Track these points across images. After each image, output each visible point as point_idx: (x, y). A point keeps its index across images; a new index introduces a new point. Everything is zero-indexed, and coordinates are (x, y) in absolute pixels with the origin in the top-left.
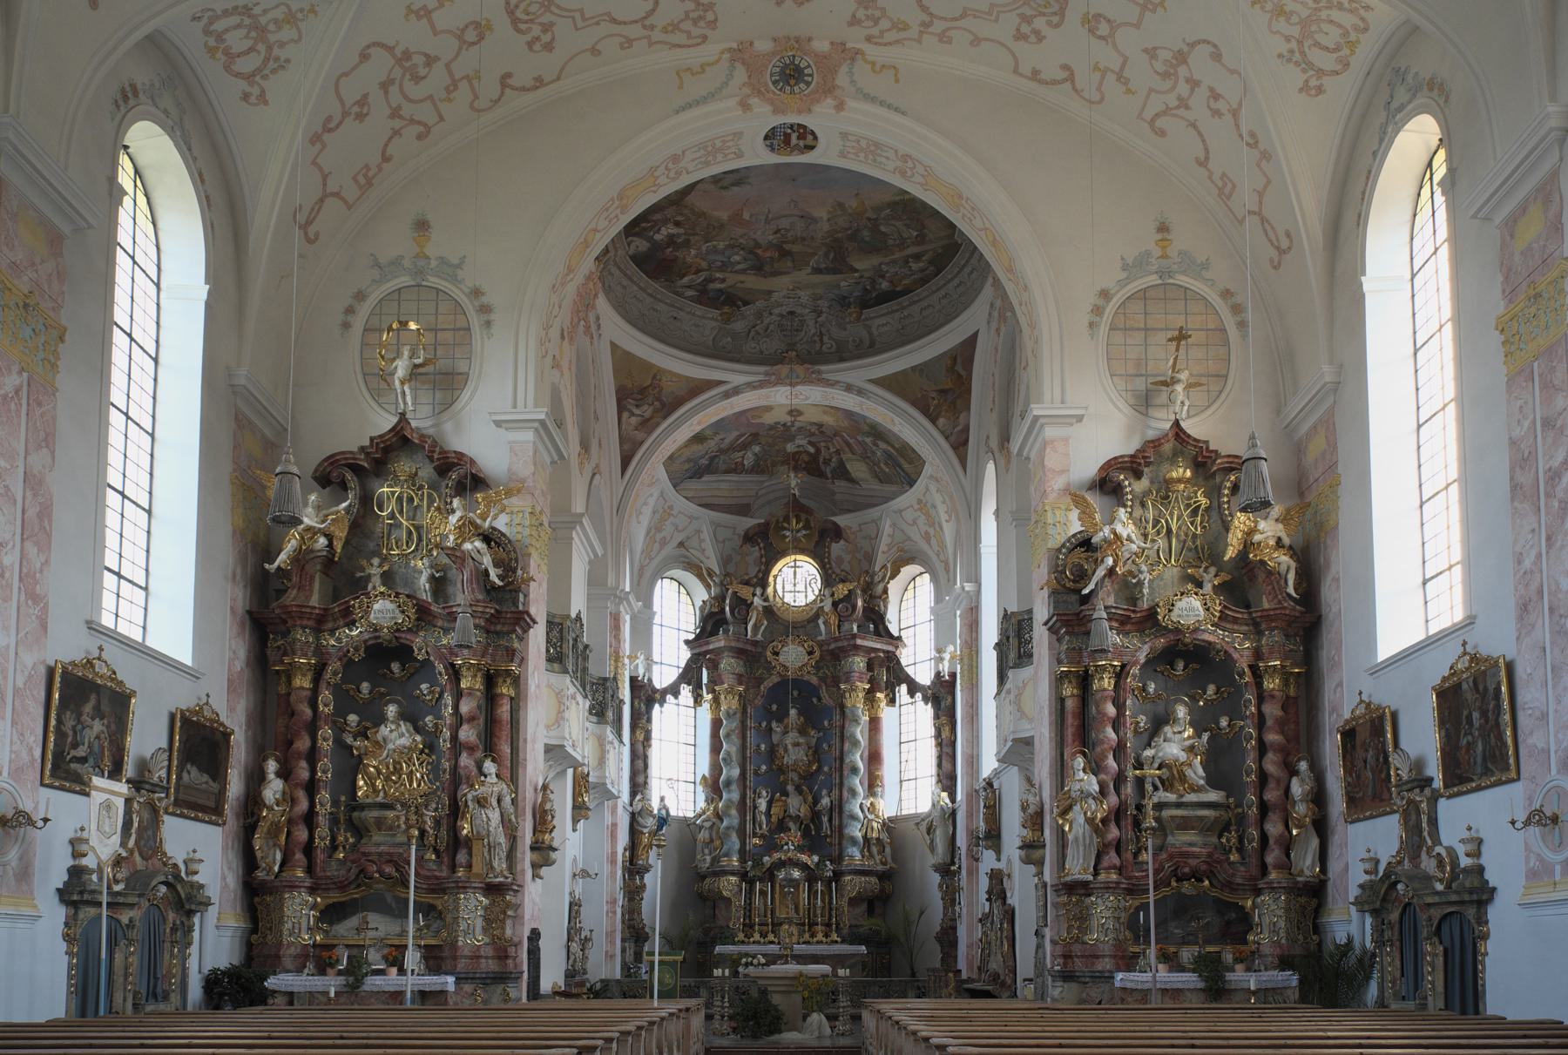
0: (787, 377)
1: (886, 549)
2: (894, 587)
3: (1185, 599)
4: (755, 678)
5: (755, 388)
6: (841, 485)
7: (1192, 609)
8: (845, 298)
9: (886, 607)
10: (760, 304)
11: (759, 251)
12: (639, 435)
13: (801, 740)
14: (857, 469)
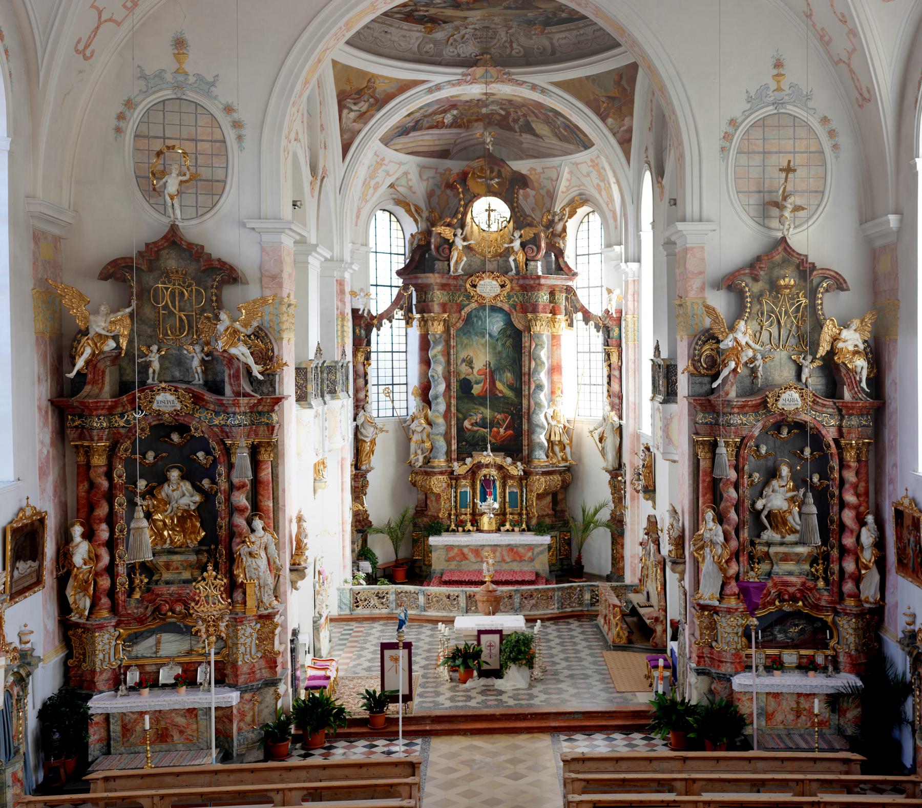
0: (482, 77)
1: (564, 189)
2: (571, 224)
3: (788, 392)
4: (457, 305)
5: (453, 85)
6: (526, 138)
7: (793, 400)
8: (531, 21)
9: (565, 246)
12: (357, 126)
14: (540, 128)
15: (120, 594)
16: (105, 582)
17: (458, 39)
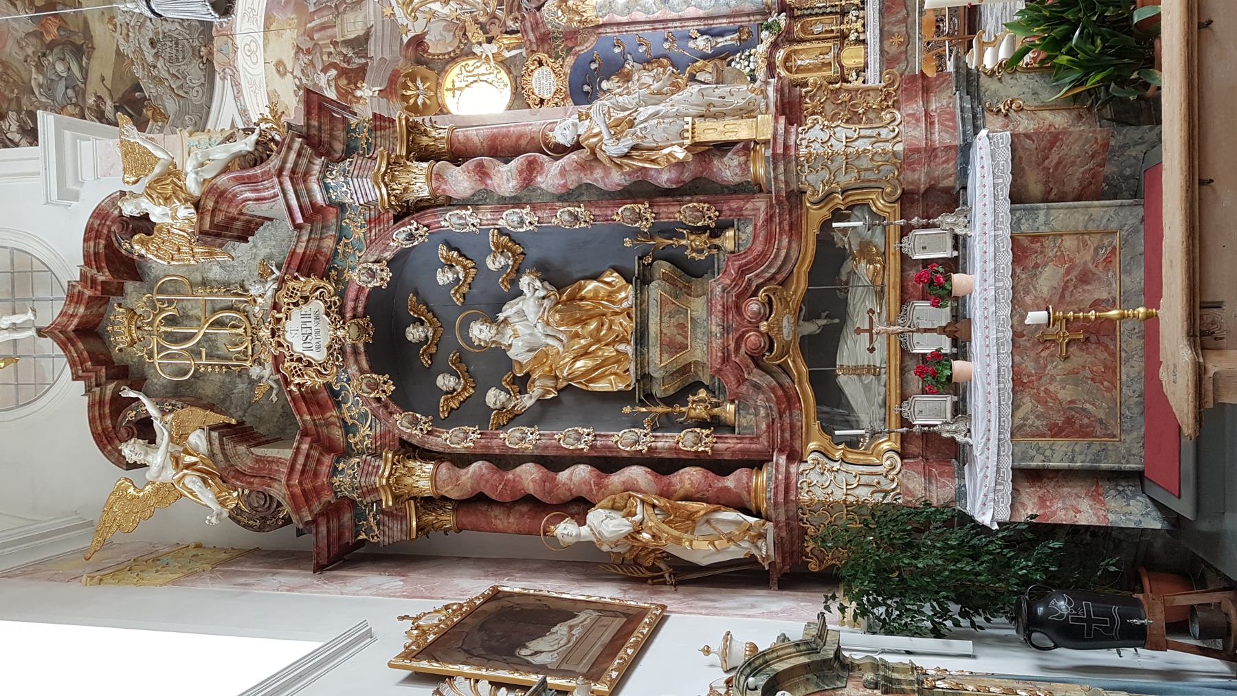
6: (373, 49)
10: (139, 72)
11: (48, 39)
15: (720, 446)
16: (690, 477)
17: (179, 83)
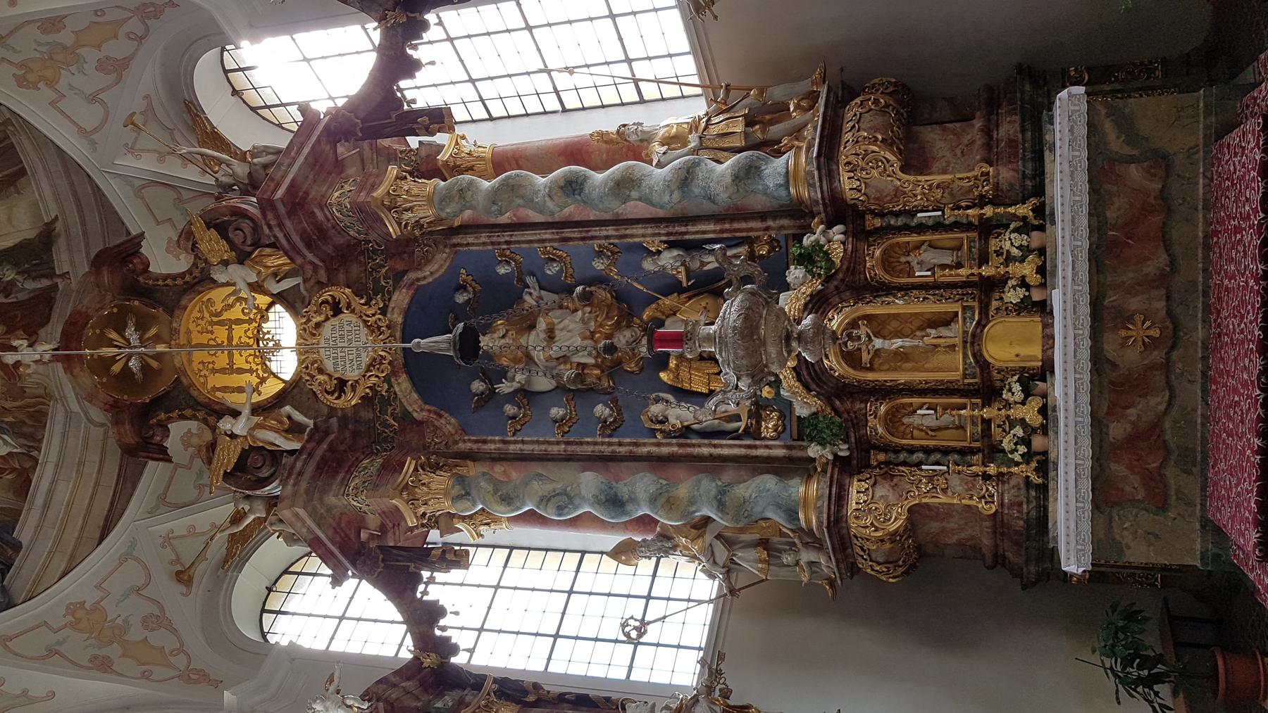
6: (62, 259)
13: (542, 324)
